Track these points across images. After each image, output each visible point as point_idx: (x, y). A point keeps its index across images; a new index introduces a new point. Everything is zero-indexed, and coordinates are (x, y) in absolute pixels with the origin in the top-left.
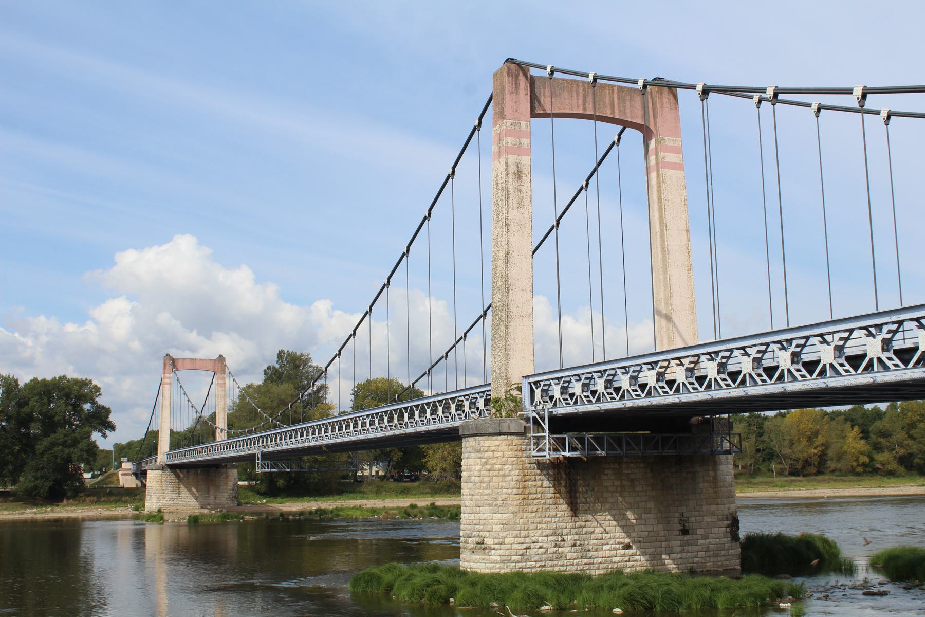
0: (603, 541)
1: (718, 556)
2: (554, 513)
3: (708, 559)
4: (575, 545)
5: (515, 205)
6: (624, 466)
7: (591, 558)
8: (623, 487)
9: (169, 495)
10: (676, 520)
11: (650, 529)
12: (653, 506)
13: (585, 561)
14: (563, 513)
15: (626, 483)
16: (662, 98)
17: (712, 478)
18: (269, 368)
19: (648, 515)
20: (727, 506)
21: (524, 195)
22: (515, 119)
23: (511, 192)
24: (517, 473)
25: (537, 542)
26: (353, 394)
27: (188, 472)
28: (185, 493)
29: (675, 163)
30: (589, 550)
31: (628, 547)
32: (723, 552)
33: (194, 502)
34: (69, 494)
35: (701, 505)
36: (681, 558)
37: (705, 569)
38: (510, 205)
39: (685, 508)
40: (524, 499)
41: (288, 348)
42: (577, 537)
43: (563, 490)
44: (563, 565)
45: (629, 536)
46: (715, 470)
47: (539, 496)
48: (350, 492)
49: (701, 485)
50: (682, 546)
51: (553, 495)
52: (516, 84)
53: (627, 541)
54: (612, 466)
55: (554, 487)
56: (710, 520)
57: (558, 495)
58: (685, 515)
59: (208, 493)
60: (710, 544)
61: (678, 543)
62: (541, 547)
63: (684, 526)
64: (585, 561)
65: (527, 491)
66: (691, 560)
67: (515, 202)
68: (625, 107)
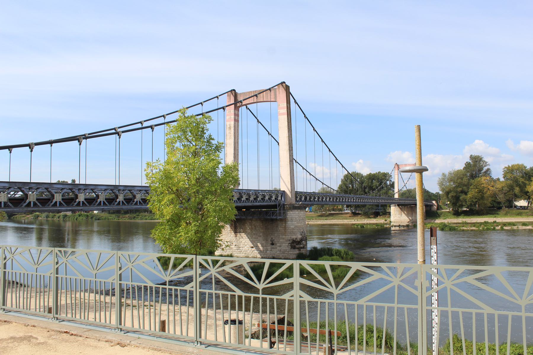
0: (245, 245)
1: (284, 253)
2: (230, 235)
3: (280, 254)
4: (236, 245)
5: (229, 138)
6: (253, 221)
7: (240, 250)
8: (252, 228)
9: (398, 216)
10: (270, 240)
13: (239, 251)
15: (253, 227)
16: (279, 90)
17: (284, 226)
18: (467, 162)
19: (260, 238)
21: (231, 134)
22: (229, 110)
23: (228, 134)
26: (503, 172)
27: (404, 207)
28: (403, 215)
29: (283, 113)
30: (240, 248)
31: (252, 247)
32: (286, 252)
33: (407, 218)
34: (381, 214)
35: (279, 236)
36: (271, 253)
37: (279, 258)
38: (227, 138)
39: (273, 236)
41: (475, 154)
42: (236, 243)
43: (233, 228)
44: (232, 251)
45: (253, 244)
46: (285, 224)
48: (491, 214)
49: (279, 228)
50: (271, 249)
51: (230, 230)
52: (230, 98)
53: (252, 246)
54: (249, 221)
55: (230, 227)
56: (282, 241)
57: (231, 230)
58: (273, 238)
59: (412, 215)
60: (281, 249)
63: (272, 242)
64: (239, 251)
66: (274, 254)
67: (229, 137)
68: (268, 96)
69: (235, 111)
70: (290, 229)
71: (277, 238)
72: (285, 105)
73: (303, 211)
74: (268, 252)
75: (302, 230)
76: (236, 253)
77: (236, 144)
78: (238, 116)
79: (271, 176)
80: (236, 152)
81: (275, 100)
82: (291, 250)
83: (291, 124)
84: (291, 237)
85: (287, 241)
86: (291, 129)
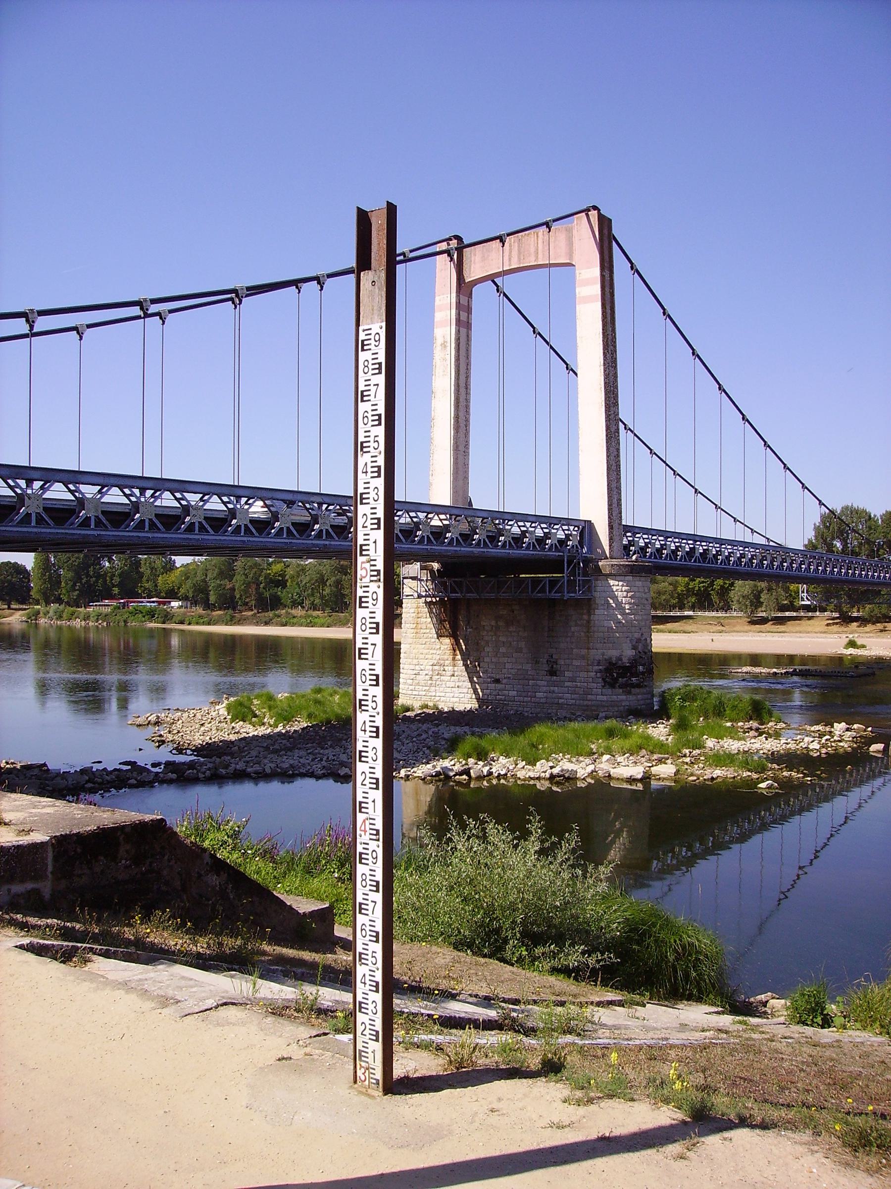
2: (438, 647)
10: (545, 661)
11: (520, 667)
12: (523, 646)
14: (446, 647)
15: (501, 623)
20: (600, 651)
24: (412, 610)
25: (424, 670)
40: (417, 633)
46: (589, 614)
47: (428, 631)
61: (545, 683)
62: (426, 675)
63: (552, 667)
65: (419, 626)
69: (458, 296)
70: (601, 629)
71: (566, 656)
72: (596, 271)
73: (643, 579)
74: (538, 695)
75: (637, 635)
76: (453, 697)
77: (462, 390)
78: (469, 310)
79: (501, 453)
80: (461, 414)
81: (568, 261)
82: (604, 690)
83: (614, 330)
84: (603, 654)
85: (592, 665)
86: (615, 342)
